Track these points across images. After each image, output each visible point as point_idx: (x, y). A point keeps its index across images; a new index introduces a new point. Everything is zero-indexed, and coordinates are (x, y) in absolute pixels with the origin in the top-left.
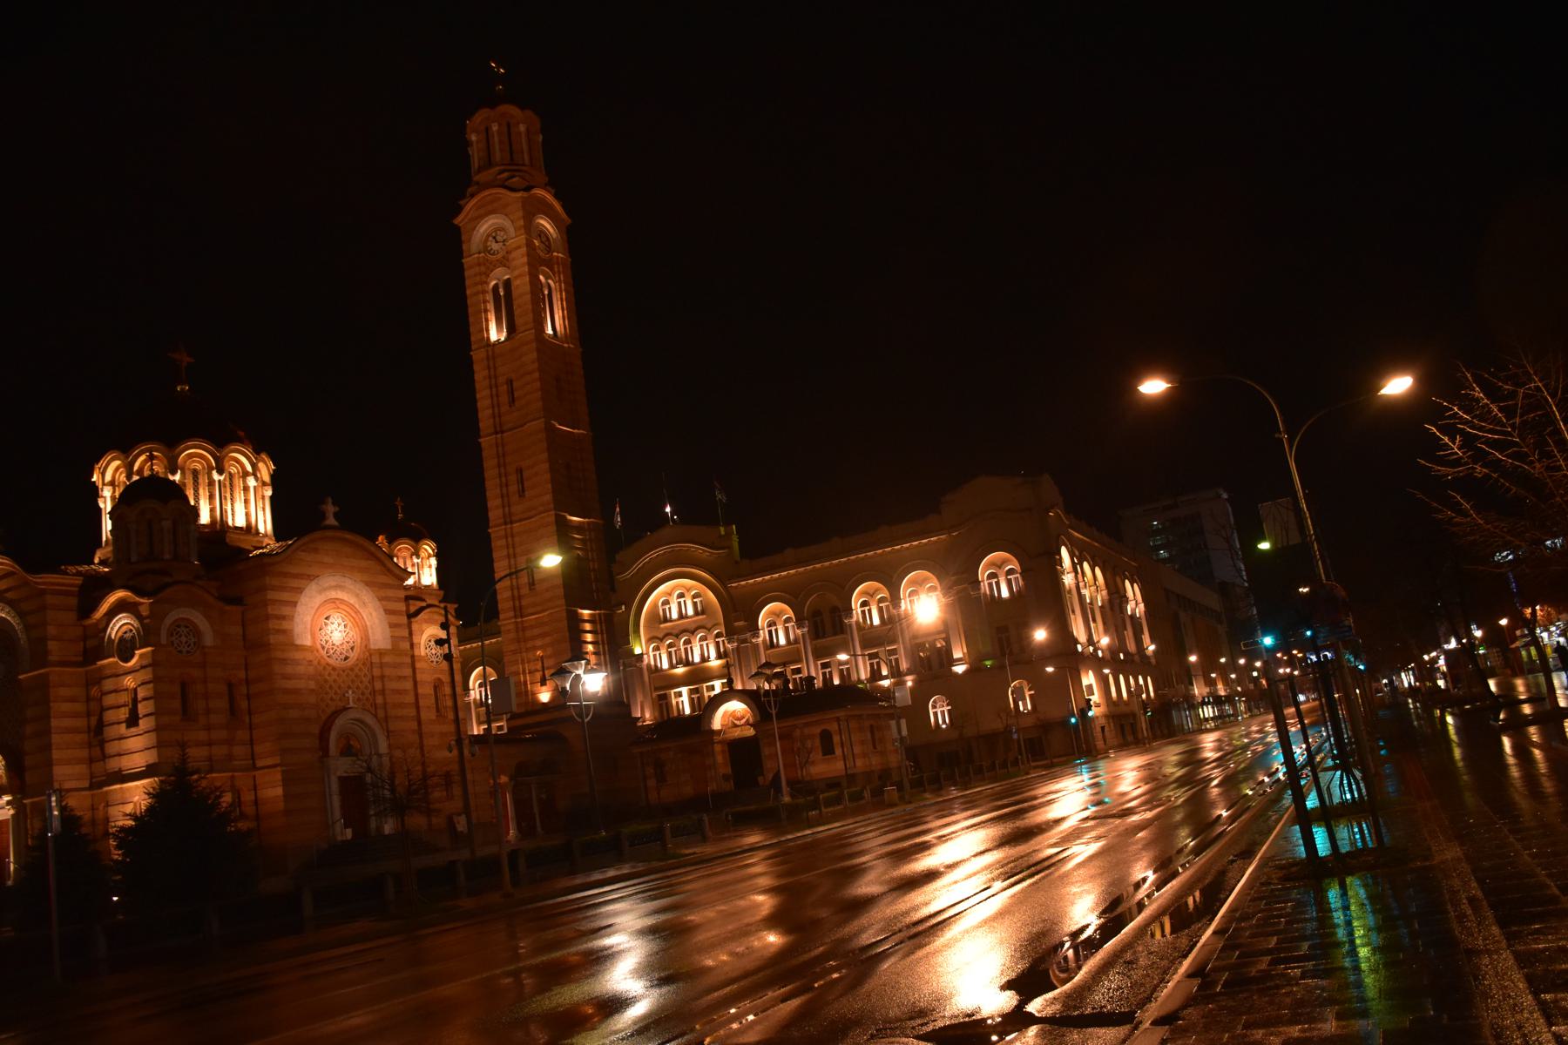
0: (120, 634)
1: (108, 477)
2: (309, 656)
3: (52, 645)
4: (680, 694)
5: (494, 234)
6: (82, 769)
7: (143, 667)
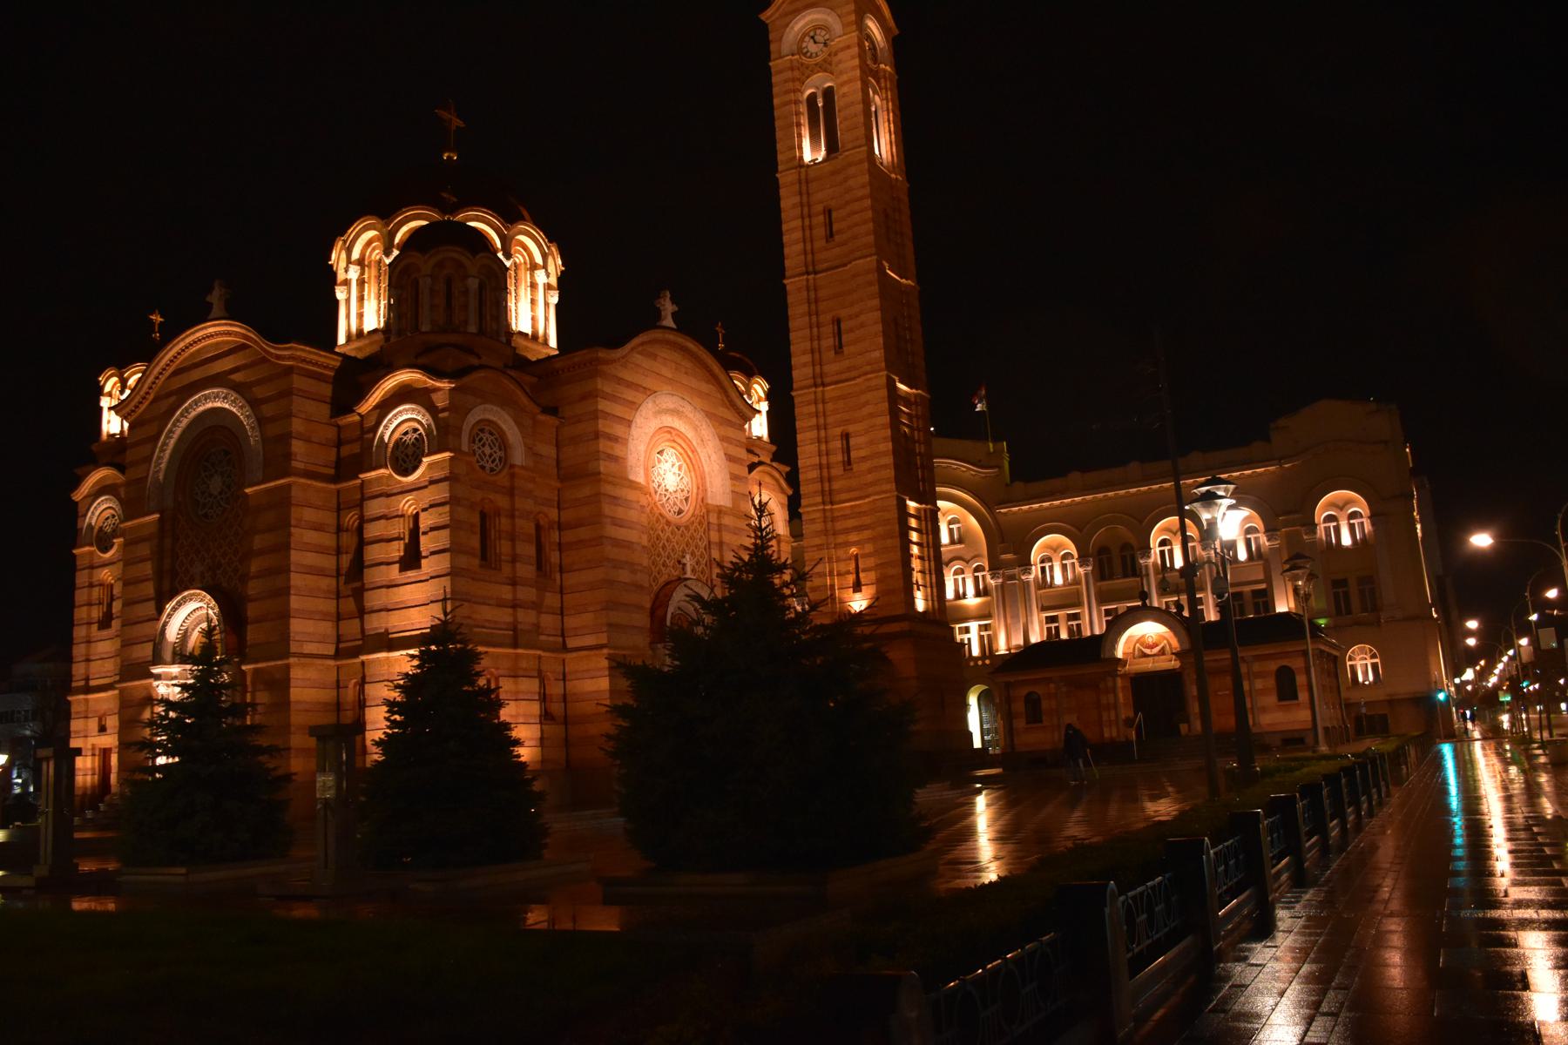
0: (397, 435)
1: (356, 255)
2: (644, 500)
3: (297, 446)
4: (967, 630)
5: (812, 34)
6: (327, 628)
7: (432, 482)
